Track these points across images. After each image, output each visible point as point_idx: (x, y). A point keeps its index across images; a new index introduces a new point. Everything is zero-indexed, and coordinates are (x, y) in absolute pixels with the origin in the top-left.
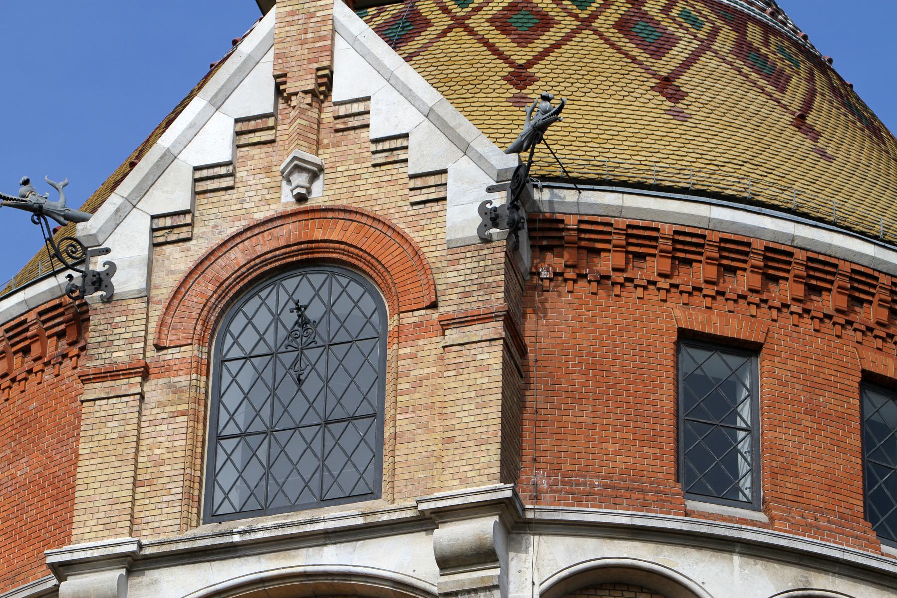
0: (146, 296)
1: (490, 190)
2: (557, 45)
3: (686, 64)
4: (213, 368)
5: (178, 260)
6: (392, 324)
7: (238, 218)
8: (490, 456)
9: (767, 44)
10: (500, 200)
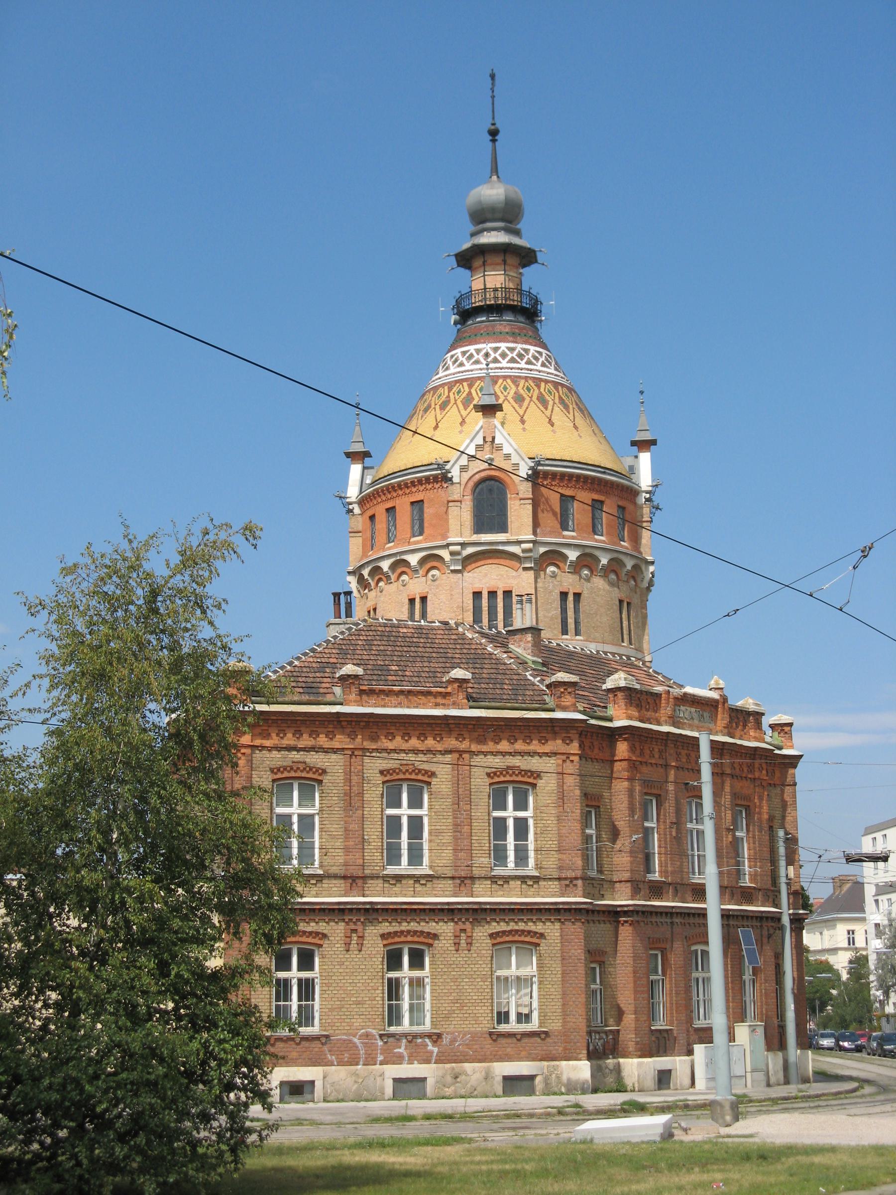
0: (460, 483)
5: (466, 476)
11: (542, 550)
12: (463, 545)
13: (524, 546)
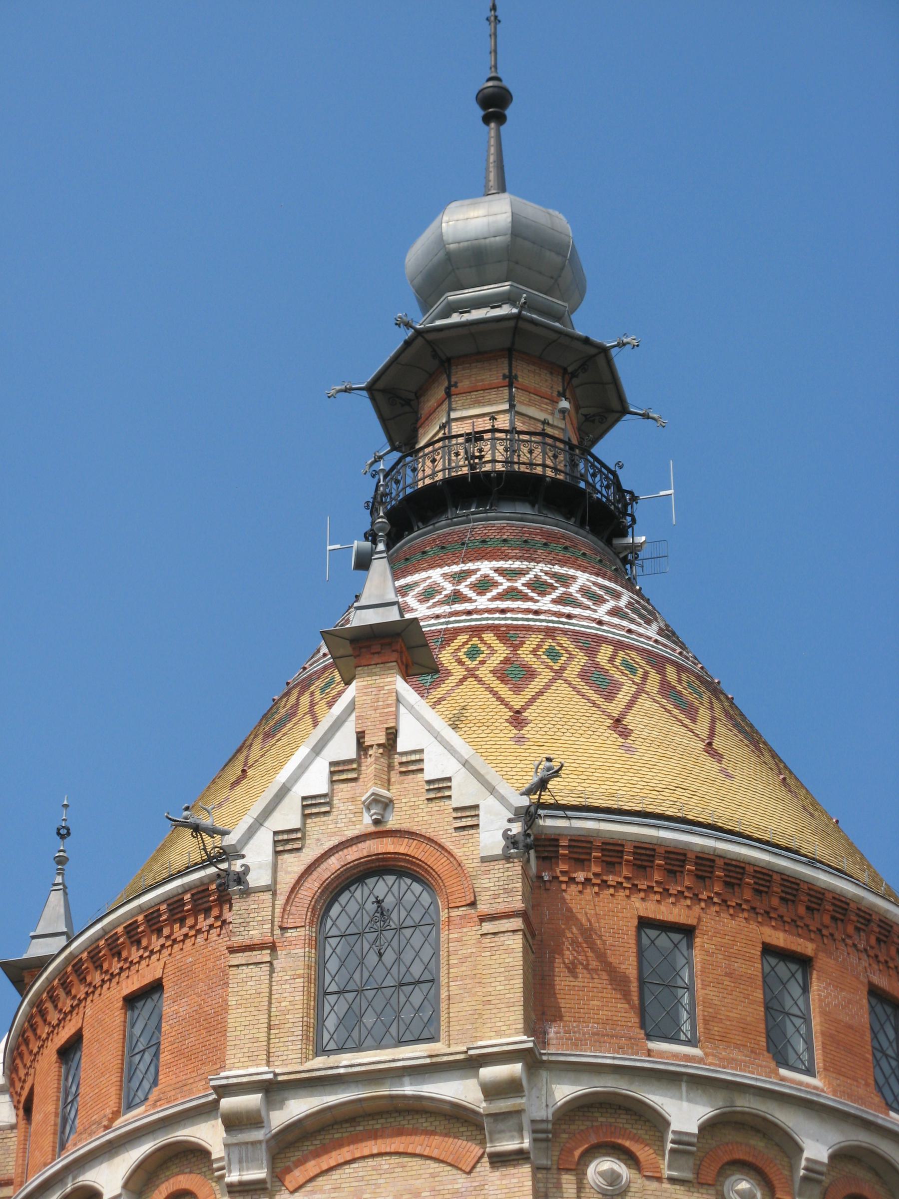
0: (271, 889)
1: (510, 821)
2: (541, 693)
3: (630, 706)
4: (319, 943)
5: (293, 865)
6: (444, 915)
7: (334, 834)
8: (516, 1015)
9: (680, 681)
10: (517, 828)
11: (564, 1091)
12: (273, 1090)
13: (489, 1073)
